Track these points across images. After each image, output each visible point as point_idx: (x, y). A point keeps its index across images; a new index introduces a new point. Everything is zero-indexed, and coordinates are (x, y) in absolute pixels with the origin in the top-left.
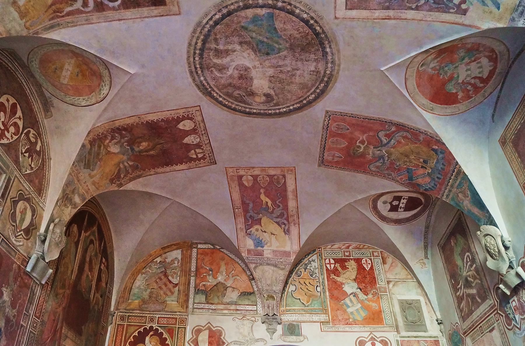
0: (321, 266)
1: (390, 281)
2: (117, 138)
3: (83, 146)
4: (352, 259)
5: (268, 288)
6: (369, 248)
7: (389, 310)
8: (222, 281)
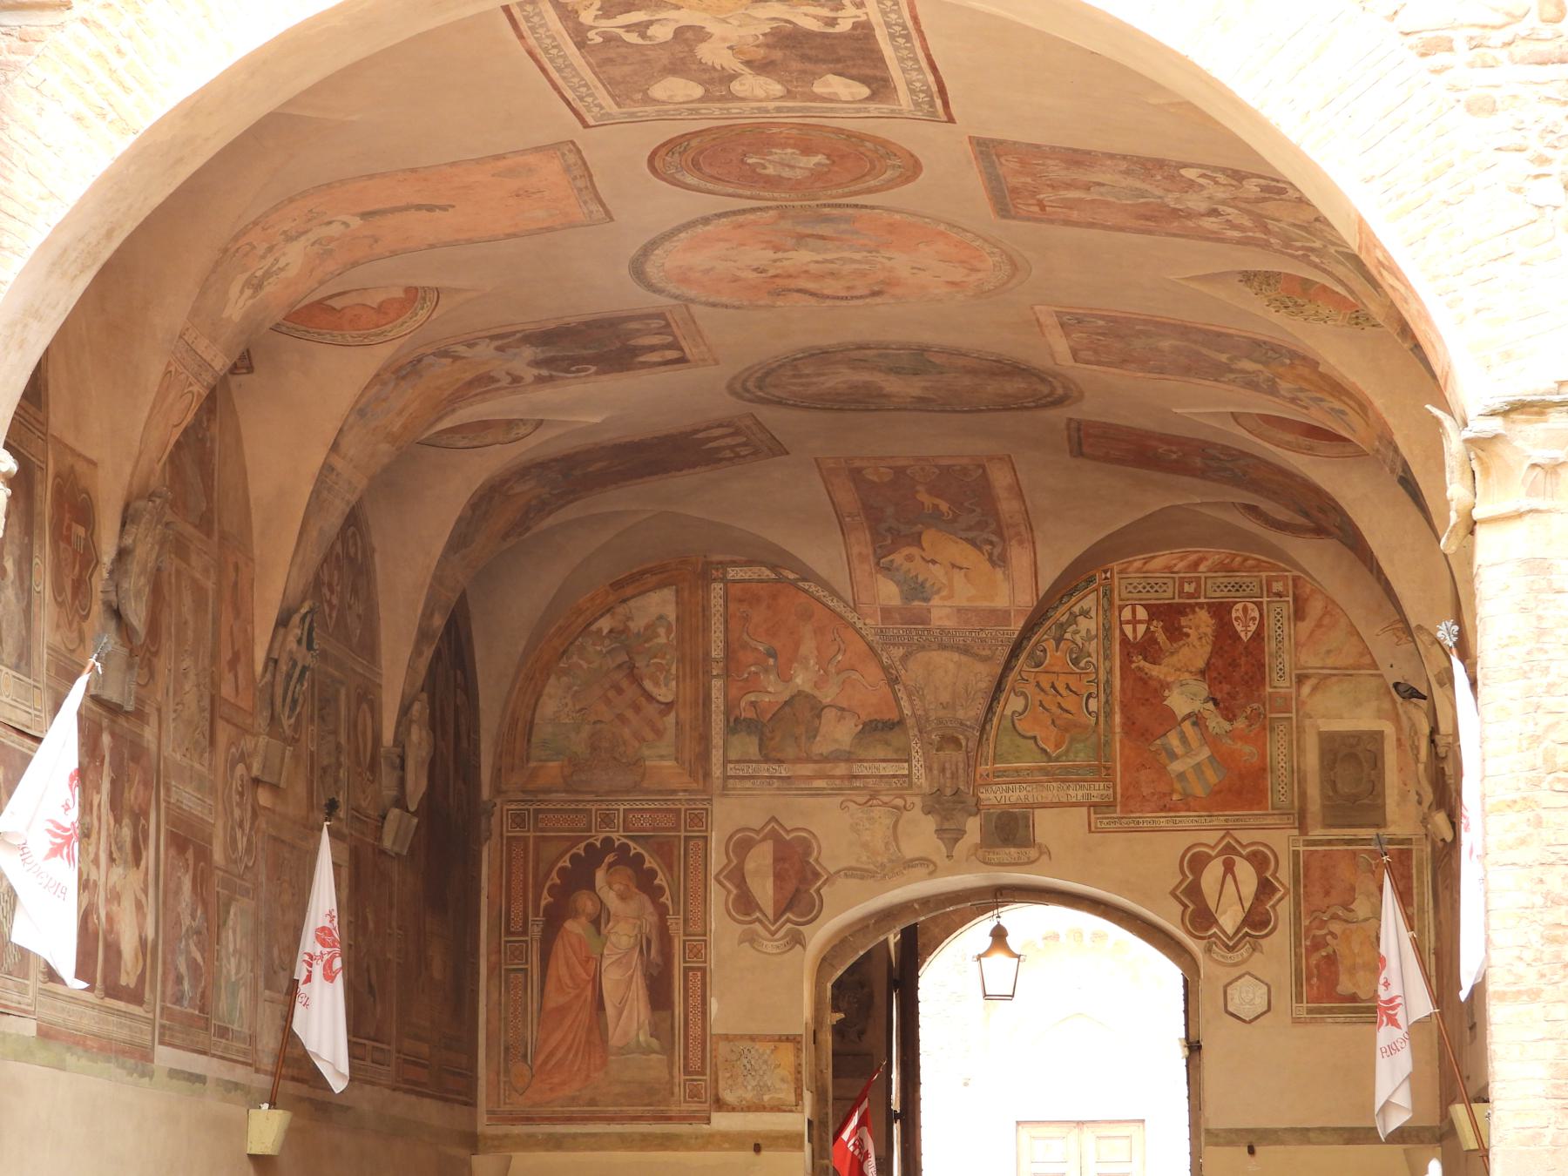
0: (1108, 631)
1: (1307, 677)
4: (1201, 605)
5: (941, 713)
6: (1259, 566)
7: (1287, 766)
8: (808, 688)
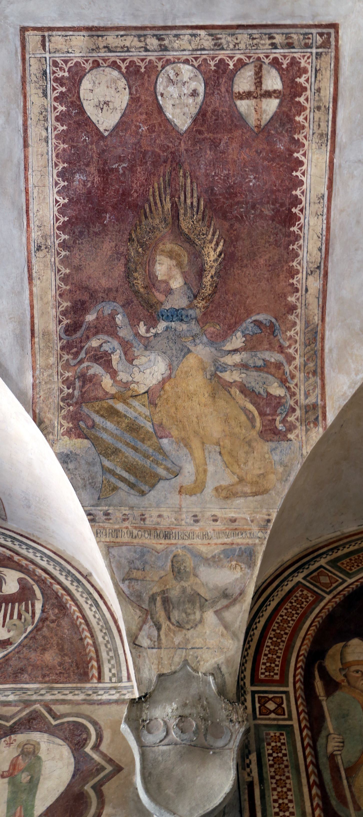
2: (106, 347)
3: (65, 459)
